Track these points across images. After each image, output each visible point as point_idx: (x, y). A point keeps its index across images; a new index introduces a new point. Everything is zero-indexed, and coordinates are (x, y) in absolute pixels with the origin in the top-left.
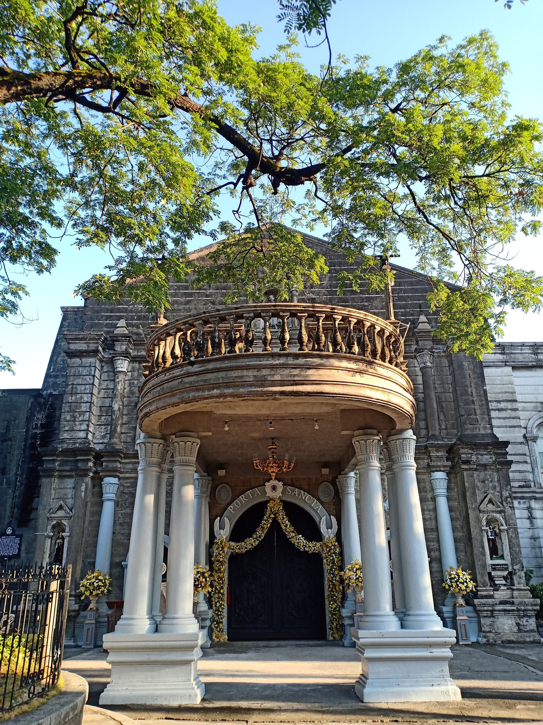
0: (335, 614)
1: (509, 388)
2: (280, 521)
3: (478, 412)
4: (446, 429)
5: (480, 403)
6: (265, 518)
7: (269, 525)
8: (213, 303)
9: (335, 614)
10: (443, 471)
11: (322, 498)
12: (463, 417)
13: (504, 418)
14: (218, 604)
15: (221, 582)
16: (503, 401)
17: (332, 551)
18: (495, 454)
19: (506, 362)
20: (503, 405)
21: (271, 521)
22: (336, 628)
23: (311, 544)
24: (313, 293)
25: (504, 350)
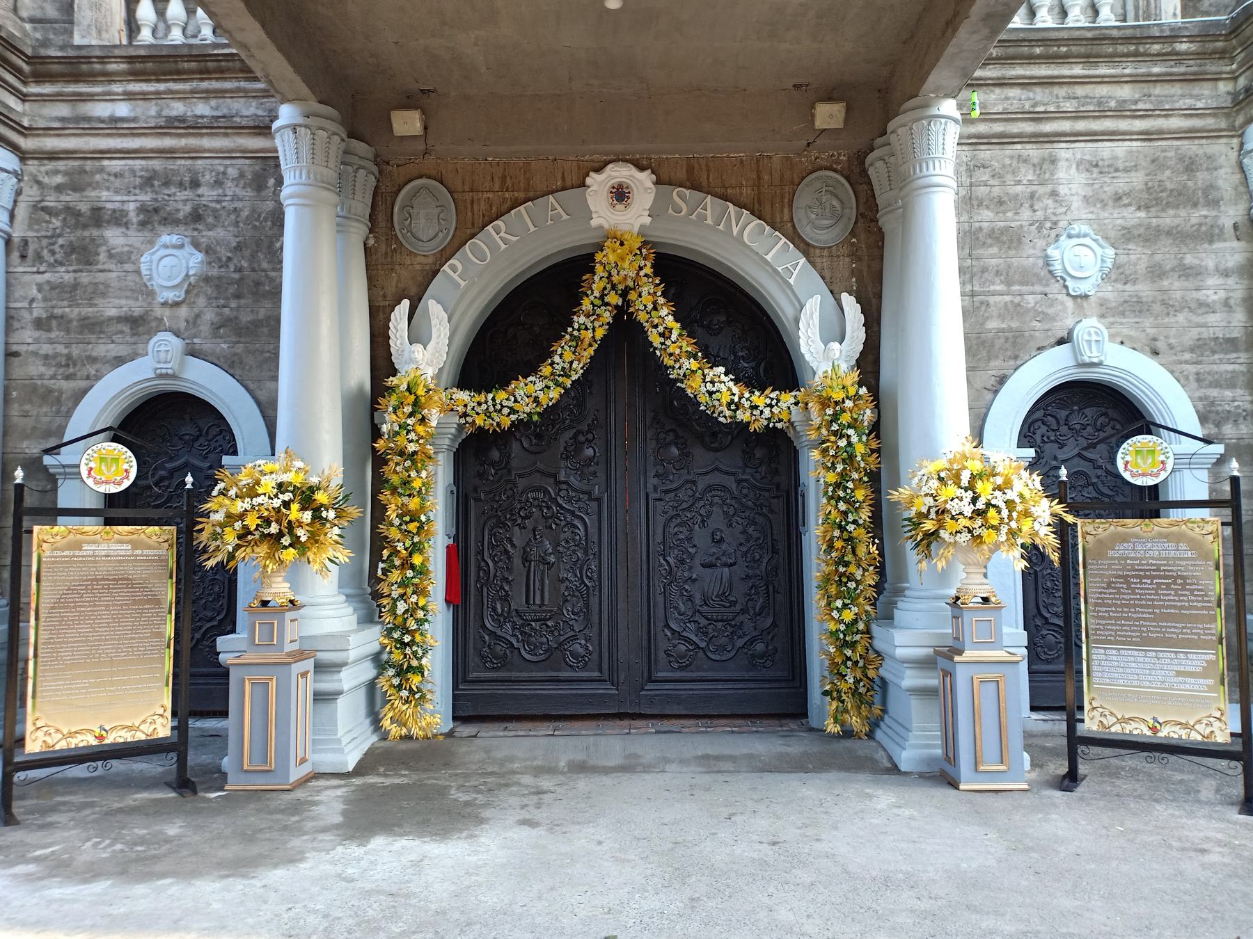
0: (852, 645)
2: (642, 317)
6: (586, 305)
7: (600, 333)
9: (852, 645)
11: (808, 233)
14: (401, 607)
15: (413, 527)
17: (845, 418)
21: (607, 317)
22: (854, 692)
23: (759, 399)
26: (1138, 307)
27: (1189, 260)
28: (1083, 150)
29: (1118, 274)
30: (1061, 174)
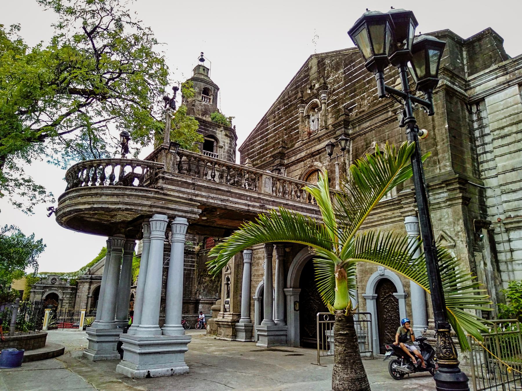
1: (514, 110)
10: (411, 215)
13: (508, 144)
16: (507, 126)
18: (449, 190)
19: (508, 82)
20: (506, 131)
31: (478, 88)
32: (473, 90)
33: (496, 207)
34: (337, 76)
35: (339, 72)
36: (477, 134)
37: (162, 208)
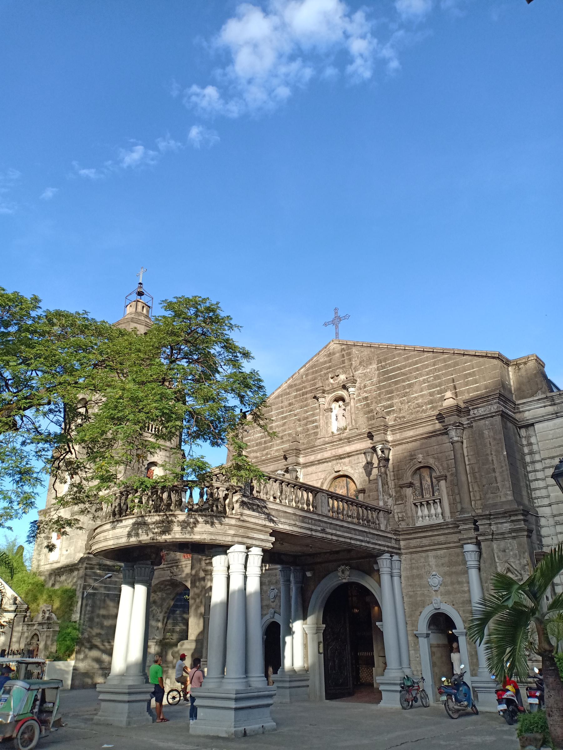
3: (499, 479)
4: (480, 500)
5: (501, 470)
8: (299, 420)
10: (471, 543)
12: (485, 487)
19: (556, 413)
24: (366, 392)
25: (553, 400)
26: (448, 593)
27: (459, 580)
28: (434, 553)
29: (443, 584)
30: (430, 560)
31: (527, 414)
32: (522, 414)
33: (550, 538)
34: (368, 370)
35: (371, 367)
36: (528, 459)
37: (243, 537)
